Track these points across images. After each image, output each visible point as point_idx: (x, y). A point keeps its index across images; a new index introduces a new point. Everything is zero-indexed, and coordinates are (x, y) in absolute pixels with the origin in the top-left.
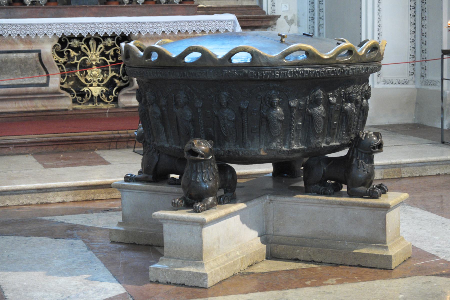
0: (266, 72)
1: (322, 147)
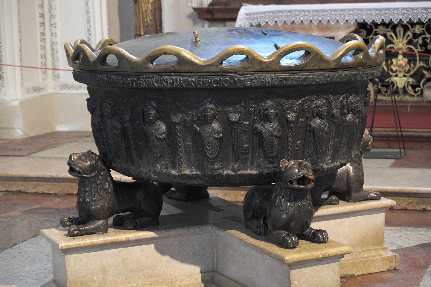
0: (131, 79)
1: (224, 175)
